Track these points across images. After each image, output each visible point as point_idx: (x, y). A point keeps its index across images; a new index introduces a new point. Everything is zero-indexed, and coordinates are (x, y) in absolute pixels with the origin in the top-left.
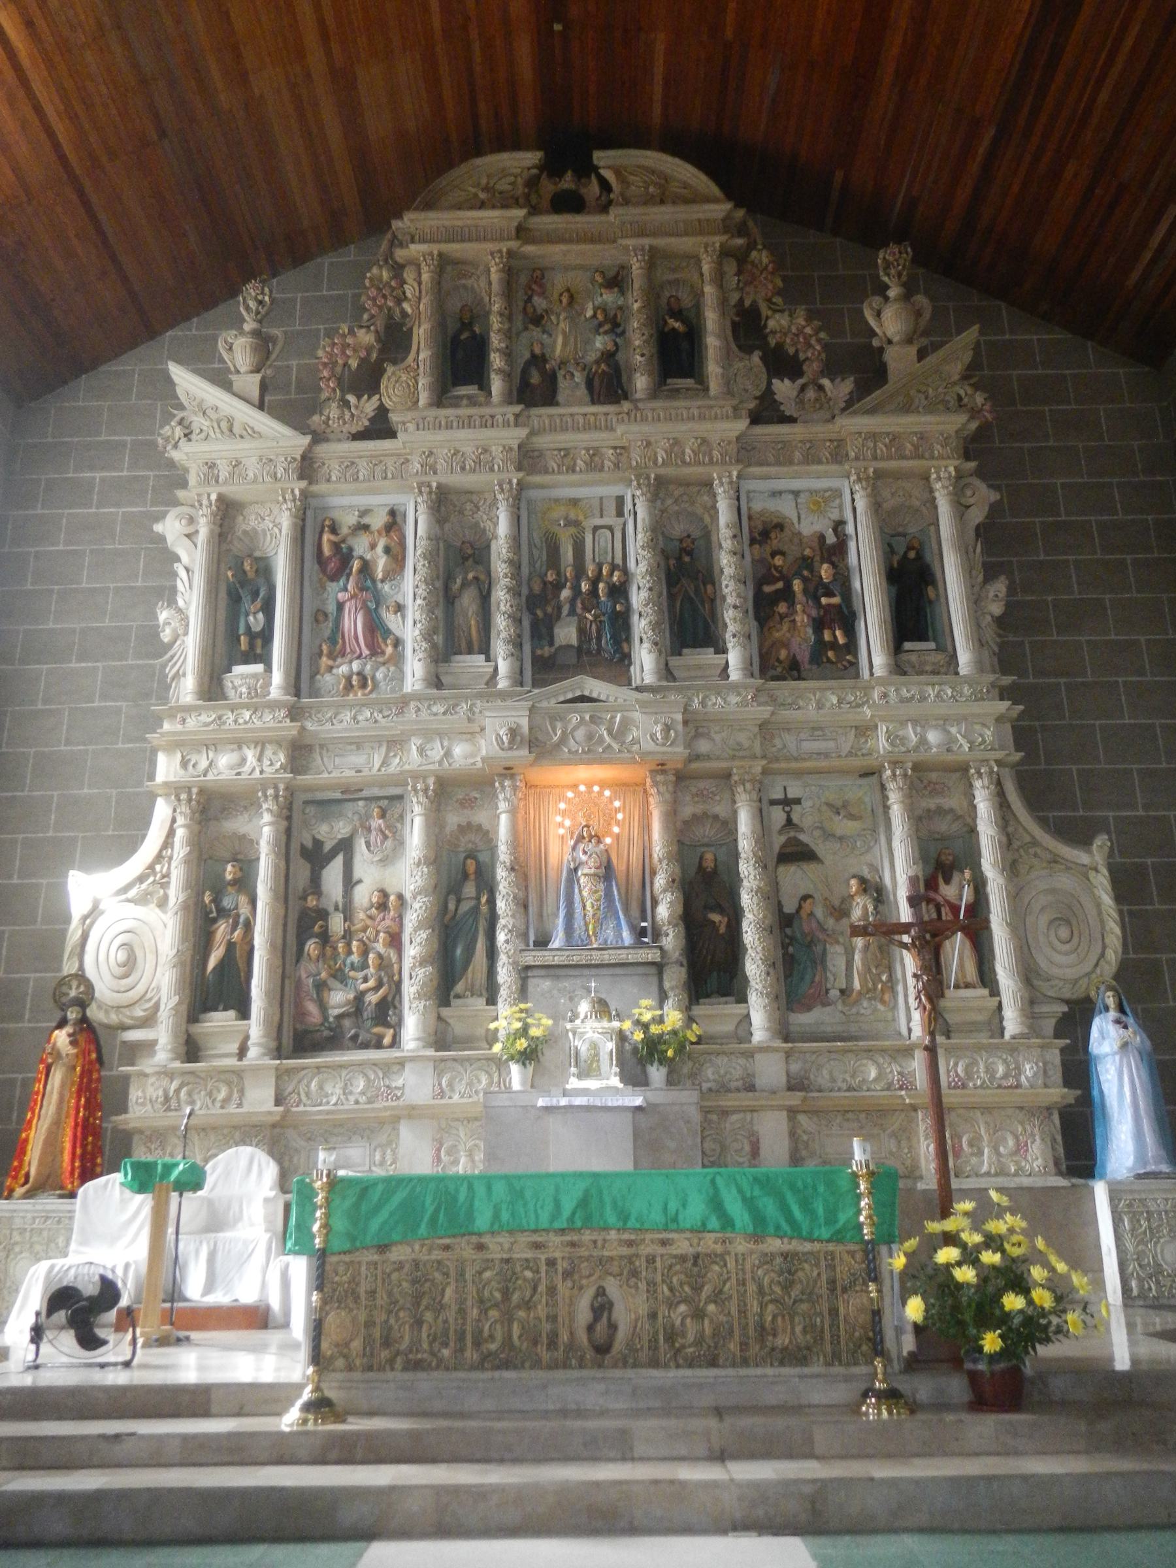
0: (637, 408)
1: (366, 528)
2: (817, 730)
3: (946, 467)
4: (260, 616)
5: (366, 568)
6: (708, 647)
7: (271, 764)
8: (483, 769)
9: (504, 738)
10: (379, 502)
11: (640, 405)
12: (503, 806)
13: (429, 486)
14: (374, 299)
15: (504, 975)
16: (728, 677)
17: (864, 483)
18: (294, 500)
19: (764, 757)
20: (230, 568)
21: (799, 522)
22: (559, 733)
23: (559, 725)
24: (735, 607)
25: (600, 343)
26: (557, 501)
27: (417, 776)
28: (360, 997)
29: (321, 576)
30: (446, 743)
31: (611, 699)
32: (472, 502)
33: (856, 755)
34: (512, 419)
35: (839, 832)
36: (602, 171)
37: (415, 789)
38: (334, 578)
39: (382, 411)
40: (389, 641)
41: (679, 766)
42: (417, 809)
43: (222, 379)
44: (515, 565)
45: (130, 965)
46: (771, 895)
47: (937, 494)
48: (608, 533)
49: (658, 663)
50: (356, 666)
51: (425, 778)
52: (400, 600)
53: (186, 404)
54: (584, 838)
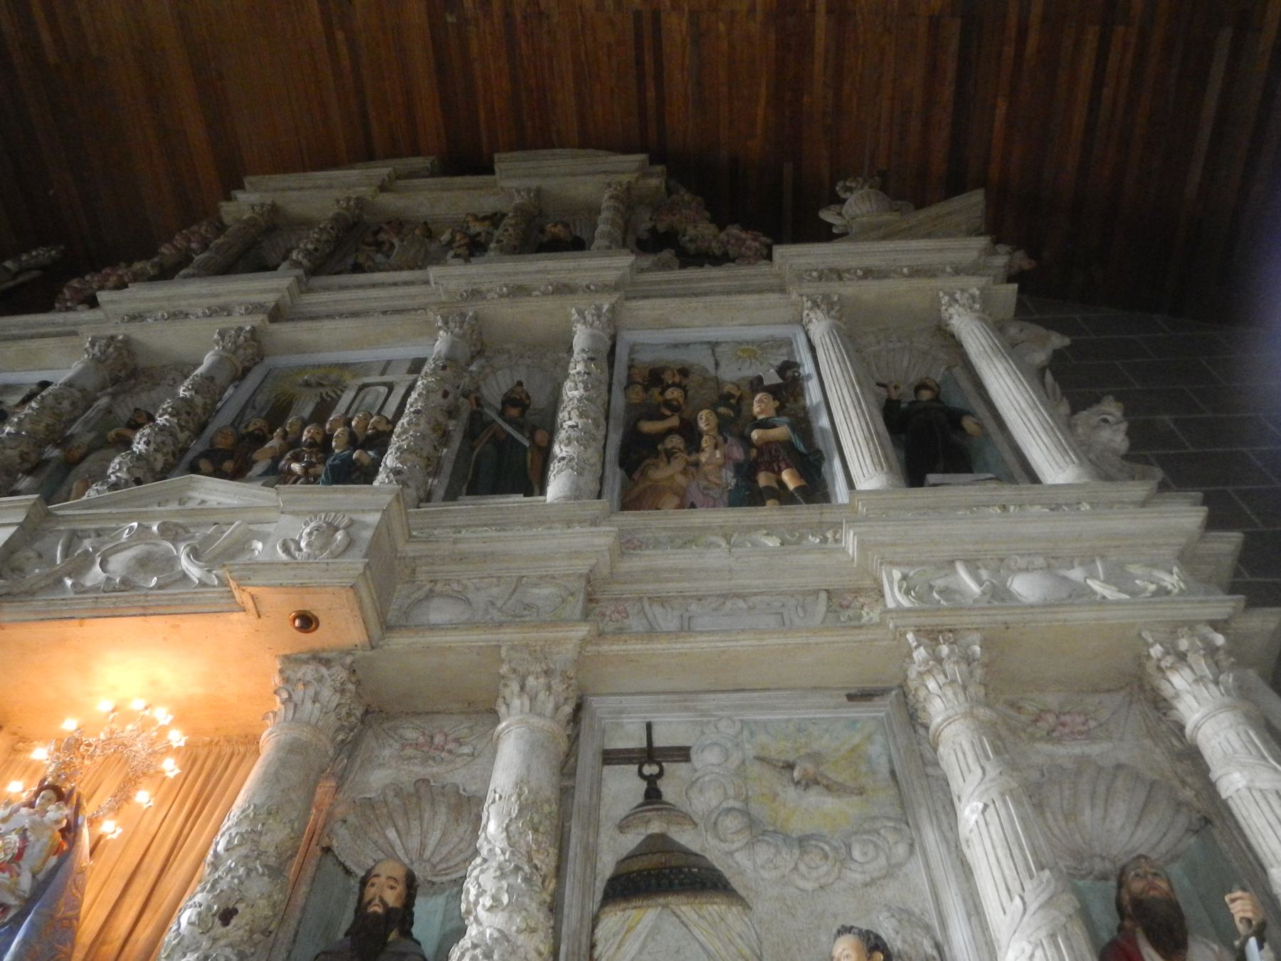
35: (797, 826)
48: (383, 390)
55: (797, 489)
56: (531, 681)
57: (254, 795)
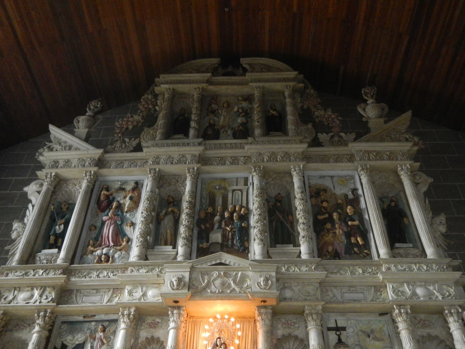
0: (255, 139)
1: (123, 189)
2: (351, 287)
3: (405, 165)
4: (62, 227)
5: (120, 207)
6: (290, 243)
7: (47, 299)
8: (162, 302)
9: (175, 283)
11: (256, 139)
12: (172, 325)
13: (155, 170)
14: (144, 105)
16: (301, 258)
17: (365, 170)
18: (90, 175)
19: (323, 300)
20: (53, 205)
21: (334, 189)
22: (206, 281)
23: (206, 277)
24: (304, 223)
25: (240, 120)
26: (216, 179)
27: (126, 306)
29: (97, 210)
30: (144, 289)
31: (237, 265)
32: (175, 179)
33: (376, 301)
34: (197, 144)
36: (244, 65)
37: (123, 315)
40: (124, 239)
41: (274, 303)
42: (123, 326)
44: (192, 205)
47: (402, 177)
48: (240, 193)
49: (263, 249)
50: (104, 251)
51: (129, 308)
52: (134, 221)
53: (53, 140)
54: (217, 346)
55: (362, 244)
56: (314, 316)
57: (265, 345)
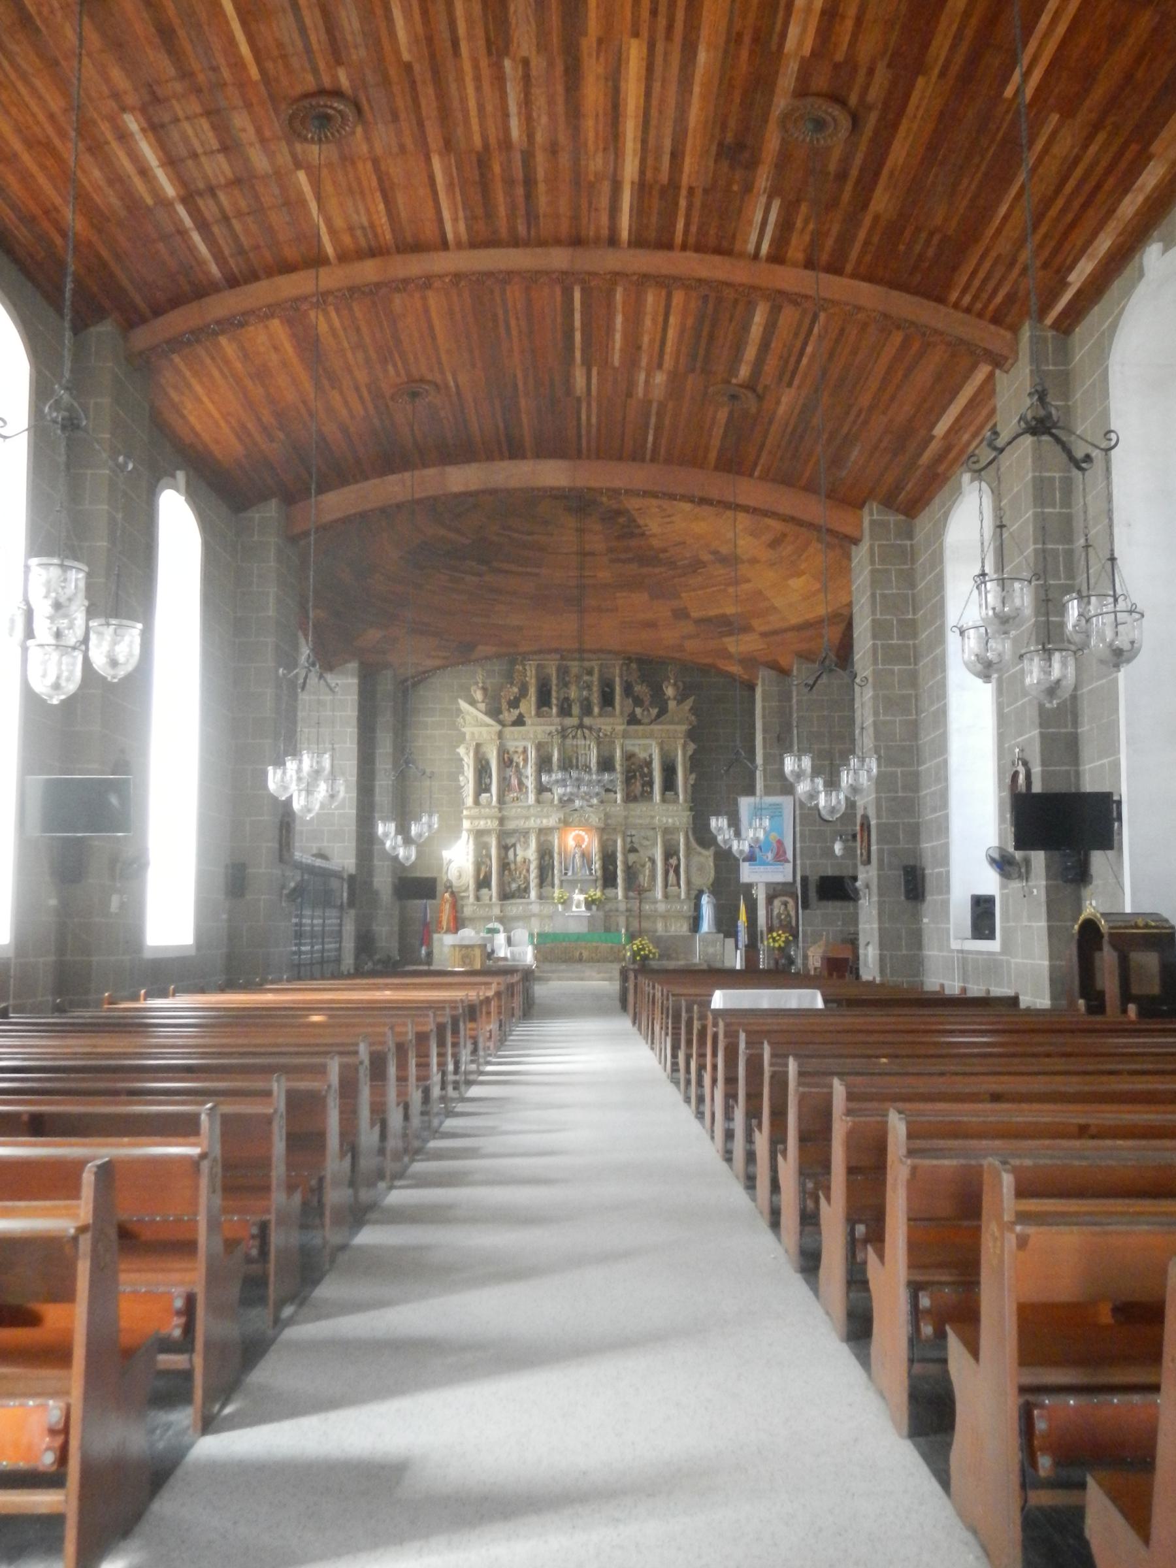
1: (516, 752)
5: (517, 765)
10: (521, 744)
12: (556, 837)
15: (557, 881)
28: (519, 886)
38: (508, 767)
39: (521, 716)
43: (473, 703)
45: (460, 876)
46: (625, 863)
